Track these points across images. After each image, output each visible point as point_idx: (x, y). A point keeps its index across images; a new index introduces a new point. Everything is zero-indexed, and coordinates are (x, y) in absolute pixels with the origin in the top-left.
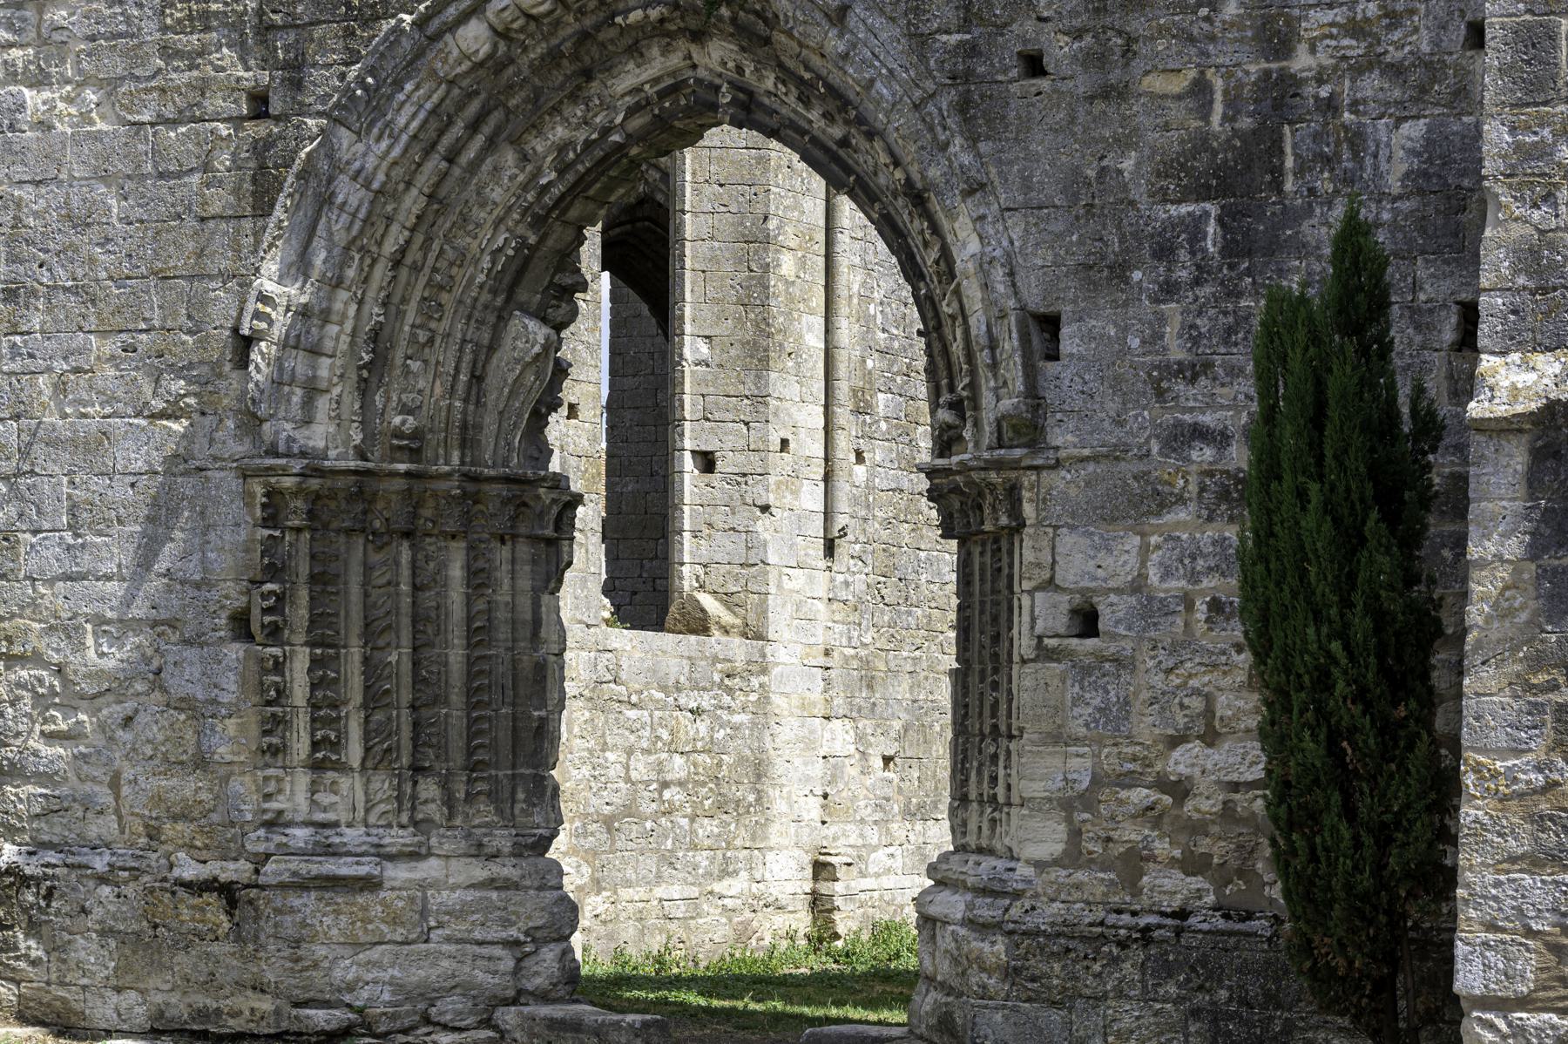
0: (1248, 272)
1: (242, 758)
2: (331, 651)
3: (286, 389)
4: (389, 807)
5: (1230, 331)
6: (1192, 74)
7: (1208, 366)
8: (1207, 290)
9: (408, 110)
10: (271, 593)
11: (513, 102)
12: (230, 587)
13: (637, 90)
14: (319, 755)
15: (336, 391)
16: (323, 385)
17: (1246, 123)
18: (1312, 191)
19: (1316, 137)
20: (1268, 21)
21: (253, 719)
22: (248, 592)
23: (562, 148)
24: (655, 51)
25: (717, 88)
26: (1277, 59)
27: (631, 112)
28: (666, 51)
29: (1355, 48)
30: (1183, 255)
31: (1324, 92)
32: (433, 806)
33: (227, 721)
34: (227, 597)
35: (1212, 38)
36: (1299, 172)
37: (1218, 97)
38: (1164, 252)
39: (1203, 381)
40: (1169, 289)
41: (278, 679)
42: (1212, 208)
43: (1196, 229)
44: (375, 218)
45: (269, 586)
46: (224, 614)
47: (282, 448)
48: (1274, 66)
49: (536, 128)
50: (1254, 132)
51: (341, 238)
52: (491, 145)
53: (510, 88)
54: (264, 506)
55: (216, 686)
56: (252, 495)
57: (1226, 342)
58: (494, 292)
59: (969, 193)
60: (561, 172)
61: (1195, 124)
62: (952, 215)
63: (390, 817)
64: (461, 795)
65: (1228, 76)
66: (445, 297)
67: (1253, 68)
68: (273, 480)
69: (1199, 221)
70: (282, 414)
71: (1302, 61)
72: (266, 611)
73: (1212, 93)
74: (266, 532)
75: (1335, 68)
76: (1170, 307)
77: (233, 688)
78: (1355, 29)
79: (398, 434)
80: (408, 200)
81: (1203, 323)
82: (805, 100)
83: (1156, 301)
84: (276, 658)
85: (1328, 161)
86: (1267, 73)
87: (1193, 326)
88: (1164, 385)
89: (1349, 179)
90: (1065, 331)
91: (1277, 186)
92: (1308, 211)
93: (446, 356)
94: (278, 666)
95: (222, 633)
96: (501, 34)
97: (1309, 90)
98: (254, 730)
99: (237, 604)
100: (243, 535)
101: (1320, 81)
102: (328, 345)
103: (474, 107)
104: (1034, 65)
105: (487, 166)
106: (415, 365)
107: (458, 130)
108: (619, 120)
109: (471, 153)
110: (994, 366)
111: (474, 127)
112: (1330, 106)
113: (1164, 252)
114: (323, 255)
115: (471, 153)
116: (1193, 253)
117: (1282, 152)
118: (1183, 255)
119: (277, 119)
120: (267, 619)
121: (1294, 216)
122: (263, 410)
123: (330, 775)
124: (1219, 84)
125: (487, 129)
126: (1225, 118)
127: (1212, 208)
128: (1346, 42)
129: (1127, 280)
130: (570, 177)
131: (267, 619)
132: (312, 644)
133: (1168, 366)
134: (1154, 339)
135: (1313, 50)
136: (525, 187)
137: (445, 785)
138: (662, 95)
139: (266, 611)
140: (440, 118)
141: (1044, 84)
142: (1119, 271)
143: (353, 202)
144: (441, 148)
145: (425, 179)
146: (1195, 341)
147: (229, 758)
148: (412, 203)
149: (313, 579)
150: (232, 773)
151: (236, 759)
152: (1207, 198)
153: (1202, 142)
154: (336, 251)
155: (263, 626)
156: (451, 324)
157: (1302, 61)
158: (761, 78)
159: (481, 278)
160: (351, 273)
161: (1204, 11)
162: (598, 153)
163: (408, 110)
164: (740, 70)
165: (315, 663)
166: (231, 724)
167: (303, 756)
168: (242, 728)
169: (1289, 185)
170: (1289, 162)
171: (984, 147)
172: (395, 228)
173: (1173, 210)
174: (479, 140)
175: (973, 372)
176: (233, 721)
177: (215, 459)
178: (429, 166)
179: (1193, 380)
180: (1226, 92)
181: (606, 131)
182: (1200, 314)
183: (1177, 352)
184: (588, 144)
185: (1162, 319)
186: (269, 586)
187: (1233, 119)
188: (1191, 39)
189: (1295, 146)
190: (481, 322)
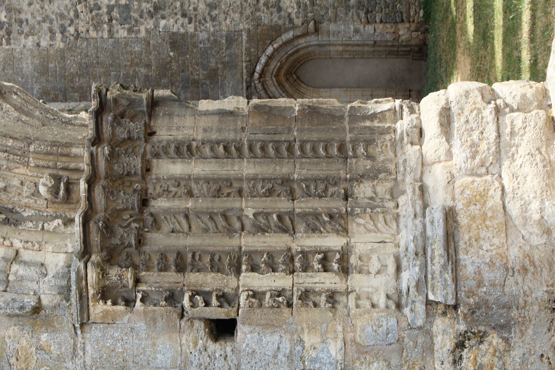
1: (340, 328)
2: (244, 258)
3: (11, 278)
4: (381, 217)
10: (191, 298)
12: (186, 339)
14: (335, 266)
15: (18, 244)
16: (11, 253)
21: (304, 315)
22: (191, 320)
32: (379, 189)
33: (307, 345)
34: (196, 344)
41: (268, 295)
45: (186, 302)
46: (212, 346)
47: (64, 283)
54: (114, 303)
55: (275, 357)
56: (106, 314)
63: (388, 217)
64: (368, 164)
68: (91, 292)
70: (35, 286)
72: (207, 304)
74: (138, 303)
77: (276, 337)
79: (55, 191)
84: (248, 296)
94: (256, 295)
95: (229, 349)
98: (315, 314)
99: (202, 333)
100: (141, 325)
120: (214, 301)
122: (30, 301)
123: (353, 260)
131: (214, 301)
132: (238, 272)
137: (360, 178)
139: (207, 304)
147: (340, 344)
149: (181, 268)
150: (354, 341)
151: (341, 336)
155: (221, 306)
165: (254, 269)
166: (309, 339)
167: (337, 279)
168: (312, 329)
176: (306, 338)
177: (74, 354)
186: (186, 302)
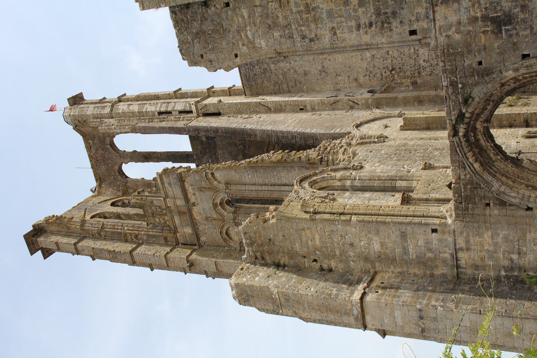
0: (514, 20)
5: (524, 22)
6: (481, 34)
7: (531, 26)
8: (517, 27)
9: (488, 177)
11: (487, 162)
13: (484, 141)
17: (489, 23)
18: (500, 10)
19: (491, 11)
20: (473, 22)
23: (494, 155)
24: (478, 137)
25: (484, 127)
26: (478, 19)
27: (488, 142)
28: (478, 135)
29: (477, 5)
30: (511, 32)
31: (484, 10)
35: (475, 31)
36: (496, 12)
37: (485, 29)
38: (511, 36)
39: (533, 26)
40: (517, 34)
42: (503, 28)
43: (507, 31)
44: (507, 185)
48: (480, 19)
49: (491, 158)
50: (491, 22)
51: (510, 191)
52: (494, 166)
53: (485, 161)
57: (526, 23)
58: (519, 168)
59: (502, 73)
60: (498, 155)
61: (489, 33)
62: (505, 77)
65: (481, 28)
66: (520, 176)
67: (480, 23)
69: (505, 29)
71: (479, 15)
73: (484, 30)
75: (480, 8)
76: (521, 34)
78: (473, 6)
80: (504, 180)
81: (523, 27)
82: (487, 109)
83: (519, 37)
85: (495, 8)
86: (481, 20)
87: (524, 29)
88: (534, 33)
89: (498, 4)
90: (525, 53)
91: (499, 17)
92: (503, 10)
93: (530, 176)
96: (476, 161)
97: (483, 13)
101: (482, 11)
102: (529, 194)
103: (488, 168)
104: (480, 63)
105: (497, 167)
106: (532, 181)
107: (492, 171)
108: (489, 144)
109: (496, 169)
110: (531, 66)
111: (491, 168)
112: (486, 9)
113: (511, 36)
114: (513, 194)
115: (496, 169)
116: (511, 31)
117: (494, 16)
118: (511, 32)
119: (490, 202)
121: (505, 13)
124: (483, 29)
125: (491, 166)
126: (488, 27)
127: (503, 28)
128: (476, 7)
129: (516, 42)
130: (499, 153)
133: (531, 33)
134: (526, 36)
135: (477, 13)
136: (501, 161)
138: (485, 136)
140: (490, 173)
141: (483, 61)
142: (515, 44)
143: (504, 188)
144: (495, 174)
145: (500, 177)
146: (526, 28)
148: (504, 179)
152: (502, 29)
153: (493, 32)
154: (512, 191)
156: (525, 175)
157: (479, 15)
158: (482, 118)
159: (516, 170)
160: (516, 190)
161: (471, 33)
162: (495, 148)
163: (488, 177)
164: (481, 122)
169: (499, 14)
170: (495, 15)
171: (494, 71)
172: (508, 182)
173: (504, 35)
174: (493, 168)
175: (532, 72)
178: (497, 176)
179: (533, 28)
180: (484, 28)
181: (491, 147)
182: (521, 28)
183: (528, 32)
184: (494, 150)
185: (522, 35)
187: (488, 26)
188: (476, 35)
189: (493, 14)
190: (524, 170)
